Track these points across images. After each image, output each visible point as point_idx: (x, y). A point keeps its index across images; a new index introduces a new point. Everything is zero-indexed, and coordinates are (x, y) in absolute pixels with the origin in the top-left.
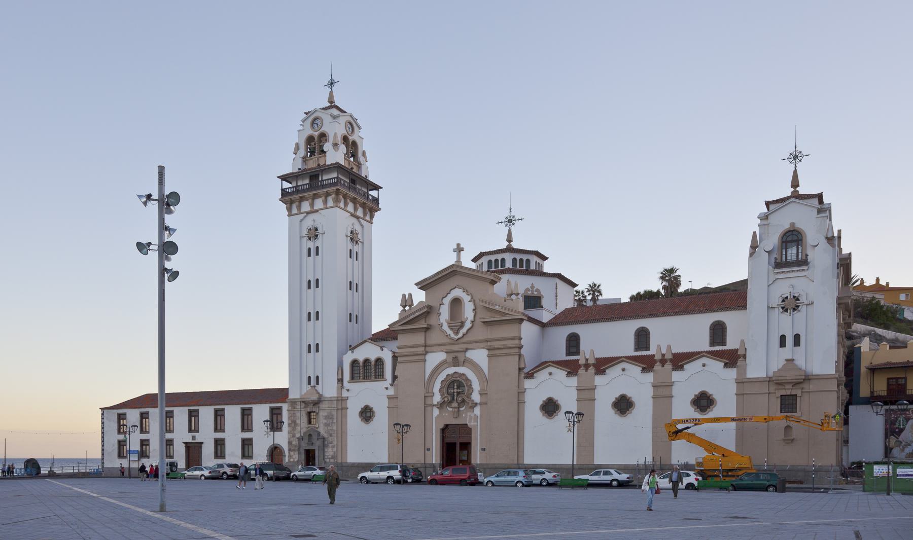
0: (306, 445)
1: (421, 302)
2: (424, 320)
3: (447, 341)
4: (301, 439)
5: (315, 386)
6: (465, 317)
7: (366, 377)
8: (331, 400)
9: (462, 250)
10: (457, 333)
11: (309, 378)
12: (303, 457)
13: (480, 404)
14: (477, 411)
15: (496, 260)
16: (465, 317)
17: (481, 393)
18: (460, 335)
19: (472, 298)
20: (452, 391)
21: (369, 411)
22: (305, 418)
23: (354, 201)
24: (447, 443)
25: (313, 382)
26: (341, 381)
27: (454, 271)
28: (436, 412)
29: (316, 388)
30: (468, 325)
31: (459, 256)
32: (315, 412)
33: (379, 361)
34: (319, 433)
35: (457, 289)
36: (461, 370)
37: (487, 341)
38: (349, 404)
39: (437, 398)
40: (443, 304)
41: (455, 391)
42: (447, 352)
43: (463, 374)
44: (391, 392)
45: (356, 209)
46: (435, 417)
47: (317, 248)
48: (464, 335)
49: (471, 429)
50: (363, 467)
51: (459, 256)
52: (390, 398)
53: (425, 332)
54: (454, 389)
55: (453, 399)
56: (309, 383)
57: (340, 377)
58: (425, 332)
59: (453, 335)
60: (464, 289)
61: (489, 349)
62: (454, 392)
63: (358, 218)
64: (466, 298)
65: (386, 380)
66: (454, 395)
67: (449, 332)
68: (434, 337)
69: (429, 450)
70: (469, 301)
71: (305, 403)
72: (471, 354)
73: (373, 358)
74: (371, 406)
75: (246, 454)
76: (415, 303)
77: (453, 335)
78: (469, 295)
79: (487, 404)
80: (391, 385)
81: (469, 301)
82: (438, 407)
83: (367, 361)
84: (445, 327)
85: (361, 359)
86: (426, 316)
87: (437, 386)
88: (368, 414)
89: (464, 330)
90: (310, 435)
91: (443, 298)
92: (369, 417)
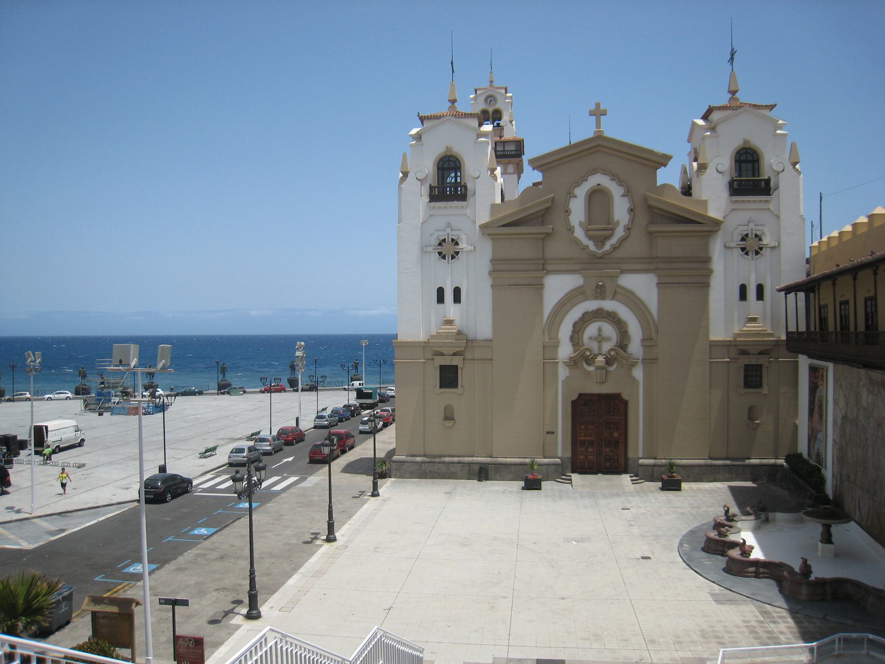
14: (638, 373)
16: (615, 220)
19: (628, 192)
27: (598, 146)
28: (563, 373)
30: (619, 232)
31: (598, 125)
36: (609, 305)
40: (576, 197)
46: (562, 381)
48: (615, 248)
51: (598, 125)
53: (543, 240)
60: (613, 176)
64: (616, 190)
67: (585, 241)
68: (556, 249)
77: (592, 247)
78: (622, 185)
81: (623, 196)
84: (579, 234)
87: (565, 330)
89: (614, 240)
91: (575, 187)
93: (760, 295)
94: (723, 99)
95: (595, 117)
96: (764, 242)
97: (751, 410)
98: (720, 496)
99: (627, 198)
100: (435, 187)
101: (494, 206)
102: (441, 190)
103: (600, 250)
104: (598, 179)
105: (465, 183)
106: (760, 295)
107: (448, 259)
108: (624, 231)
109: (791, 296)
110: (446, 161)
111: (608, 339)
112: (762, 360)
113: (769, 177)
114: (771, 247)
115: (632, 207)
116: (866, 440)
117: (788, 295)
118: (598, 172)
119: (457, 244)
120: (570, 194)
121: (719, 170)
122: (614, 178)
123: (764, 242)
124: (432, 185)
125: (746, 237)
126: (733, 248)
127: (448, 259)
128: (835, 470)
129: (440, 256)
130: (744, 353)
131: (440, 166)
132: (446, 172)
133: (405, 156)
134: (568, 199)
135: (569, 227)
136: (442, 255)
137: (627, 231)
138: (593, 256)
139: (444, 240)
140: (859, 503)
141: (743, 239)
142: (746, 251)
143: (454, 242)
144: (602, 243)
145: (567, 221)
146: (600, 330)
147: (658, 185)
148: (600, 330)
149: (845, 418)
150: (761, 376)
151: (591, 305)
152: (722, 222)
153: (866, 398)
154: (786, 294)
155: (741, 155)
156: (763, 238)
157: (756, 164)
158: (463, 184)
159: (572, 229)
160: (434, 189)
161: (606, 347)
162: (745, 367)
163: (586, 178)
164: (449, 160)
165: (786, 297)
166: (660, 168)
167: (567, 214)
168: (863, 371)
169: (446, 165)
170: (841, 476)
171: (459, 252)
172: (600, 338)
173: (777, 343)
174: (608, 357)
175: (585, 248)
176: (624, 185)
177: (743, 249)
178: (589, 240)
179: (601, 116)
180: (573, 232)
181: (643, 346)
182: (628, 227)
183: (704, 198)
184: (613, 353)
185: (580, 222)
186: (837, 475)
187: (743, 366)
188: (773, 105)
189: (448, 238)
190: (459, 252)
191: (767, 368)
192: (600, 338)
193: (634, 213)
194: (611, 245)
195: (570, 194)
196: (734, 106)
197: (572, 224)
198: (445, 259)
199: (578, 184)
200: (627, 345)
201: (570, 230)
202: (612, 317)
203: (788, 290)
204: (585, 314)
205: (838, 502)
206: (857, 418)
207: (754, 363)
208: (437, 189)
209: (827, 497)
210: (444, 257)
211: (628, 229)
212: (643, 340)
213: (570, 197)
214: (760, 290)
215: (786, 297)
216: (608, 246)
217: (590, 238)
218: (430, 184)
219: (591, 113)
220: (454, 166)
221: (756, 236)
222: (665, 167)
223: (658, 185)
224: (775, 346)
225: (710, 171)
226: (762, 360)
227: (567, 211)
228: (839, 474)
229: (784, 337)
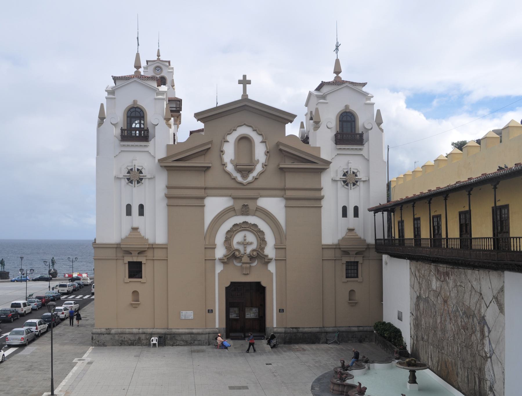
2: (203, 156)
3: (233, 184)
9: (249, 82)
10: (244, 177)
13: (276, 260)
14: (272, 267)
16: (256, 158)
17: (277, 247)
18: (250, 178)
19: (265, 140)
27: (245, 105)
30: (259, 168)
36: (252, 220)
37: (284, 189)
40: (228, 142)
42: (234, 198)
43: (255, 226)
59: (239, 179)
61: (287, 199)
70: (262, 142)
72: (265, 203)
77: (239, 179)
81: (262, 142)
84: (230, 168)
86: (206, 152)
89: (255, 174)
93: (356, 214)
94: (330, 77)
95: (242, 85)
96: (359, 177)
97: (352, 292)
98: (333, 353)
99: (264, 144)
100: (125, 130)
101: (168, 146)
102: (129, 132)
103: (245, 180)
104: (244, 131)
105: (148, 128)
106: (356, 214)
107: (135, 183)
108: (263, 167)
109: (379, 214)
110: (134, 111)
111: (251, 243)
112: (359, 259)
113: (362, 132)
114: (363, 181)
115: (268, 151)
116: (436, 312)
117: (376, 214)
119: (141, 172)
120: (224, 139)
121: (329, 127)
123: (359, 177)
124: (123, 128)
125: (346, 174)
126: (337, 181)
127: (135, 183)
128: (413, 333)
129: (128, 181)
130: (346, 253)
131: (129, 115)
132: (133, 120)
133: (102, 105)
135: (223, 163)
136: (130, 180)
137: (264, 166)
138: (241, 183)
139: (132, 169)
140: (431, 355)
141: (344, 175)
142: (346, 183)
143: (139, 171)
144: (247, 175)
145: (221, 159)
146: (245, 237)
147: (286, 136)
148: (245, 237)
149: (419, 298)
150: (357, 270)
151: (239, 219)
152: (330, 163)
153: (435, 284)
154: (375, 213)
155: (343, 117)
156: (358, 174)
157: (353, 123)
158: (145, 128)
159: (226, 165)
160: (124, 131)
161: (249, 249)
162: (346, 264)
164: (135, 111)
165: (375, 215)
166: (287, 123)
168: (432, 266)
169: (133, 114)
170: (417, 337)
171: (142, 179)
172: (245, 244)
173: (368, 247)
174: (251, 256)
175: (234, 179)
176: (263, 134)
177: (344, 182)
178: (237, 173)
179: (247, 85)
180: (226, 167)
181: (276, 248)
183: (318, 146)
184: (255, 253)
185: (232, 162)
186: (414, 336)
187: (345, 263)
188: (365, 83)
189: (135, 168)
190: (142, 179)
191: (361, 263)
192: (245, 244)
193: (269, 154)
194: (253, 177)
195: (224, 139)
196: (338, 82)
198: (132, 184)
202: (254, 229)
203: (376, 210)
204: (235, 225)
205: (415, 354)
206: (428, 297)
207: (352, 260)
208: (126, 131)
209: (407, 352)
210: (131, 182)
211: (265, 165)
212: (275, 245)
214: (356, 209)
215: (375, 215)
216: (250, 178)
217: (239, 171)
218: (122, 128)
219: (240, 82)
220: (139, 115)
221: (354, 173)
222: (291, 123)
223: (286, 135)
224: (366, 248)
225: (323, 127)
226: (359, 259)
227: (222, 151)
228: (415, 336)
229: (373, 242)
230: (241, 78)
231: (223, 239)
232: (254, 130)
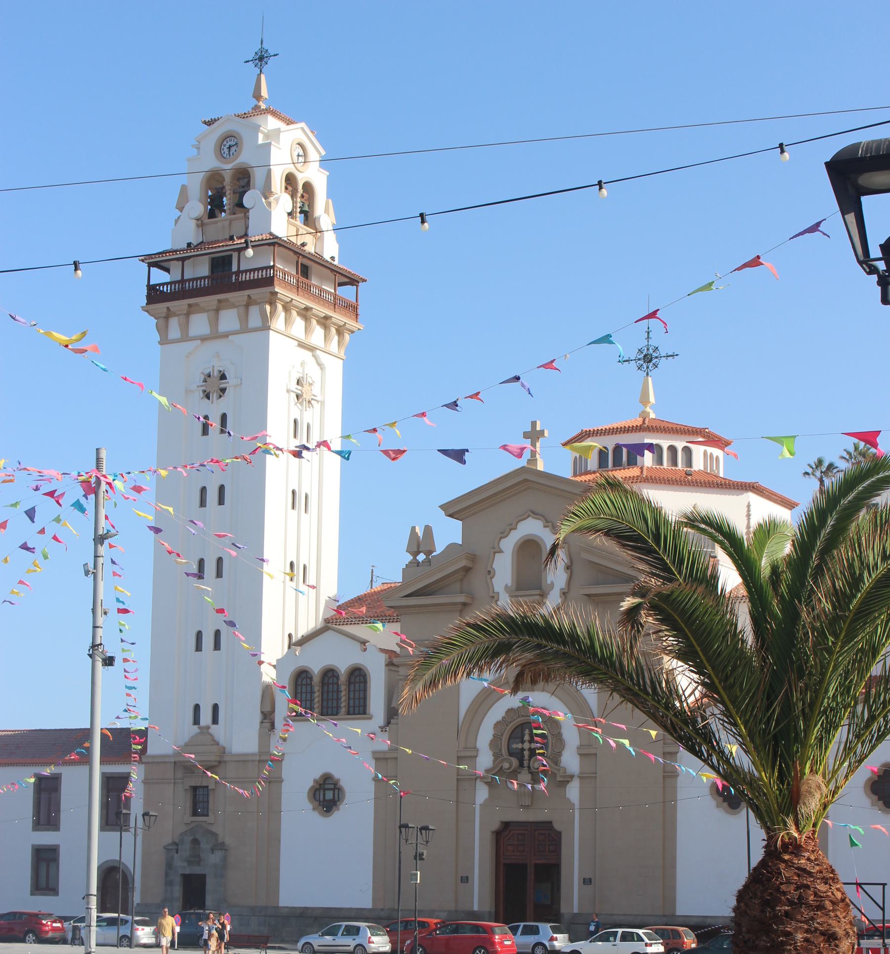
0: (185, 864)
1: (452, 547)
4: (174, 847)
5: (208, 728)
6: (549, 582)
7: (329, 710)
8: (243, 760)
11: (197, 708)
12: (177, 891)
14: (573, 792)
15: (618, 449)
16: (549, 582)
20: (520, 746)
21: (332, 786)
22: (184, 802)
23: (305, 313)
24: (506, 865)
25: (206, 718)
26: (268, 717)
27: (526, 480)
28: (482, 793)
29: (210, 731)
32: (207, 787)
33: (358, 675)
34: (215, 835)
35: (530, 519)
38: (287, 770)
39: (485, 760)
40: (501, 551)
41: (526, 746)
44: (383, 743)
45: (308, 329)
47: (224, 417)
49: (560, 833)
50: (316, 918)
52: (380, 758)
54: (523, 742)
55: (521, 765)
56: (196, 721)
57: (268, 709)
58: (461, 611)
62: (523, 750)
63: (311, 349)
65: (370, 718)
66: (523, 756)
69: (465, 880)
71: (188, 768)
73: (343, 667)
74: (336, 775)
75: (43, 883)
76: (440, 548)
79: (596, 777)
80: (382, 728)
82: (486, 783)
83: (329, 673)
85: (316, 669)
88: (329, 795)
90: (196, 842)
91: (501, 538)
92: (330, 801)
118: (529, 516)
120: (494, 548)
122: (548, 524)
134: (492, 553)
135: (491, 594)
145: (489, 586)
163: (513, 526)
167: (488, 577)
182: (564, 591)
195: (494, 548)
197: (496, 589)
199: (504, 535)
200: (560, 754)
201: (493, 597)
213: (495, 553)
230: (529, 429)
231: (490, 737)
232: (545, 527)
